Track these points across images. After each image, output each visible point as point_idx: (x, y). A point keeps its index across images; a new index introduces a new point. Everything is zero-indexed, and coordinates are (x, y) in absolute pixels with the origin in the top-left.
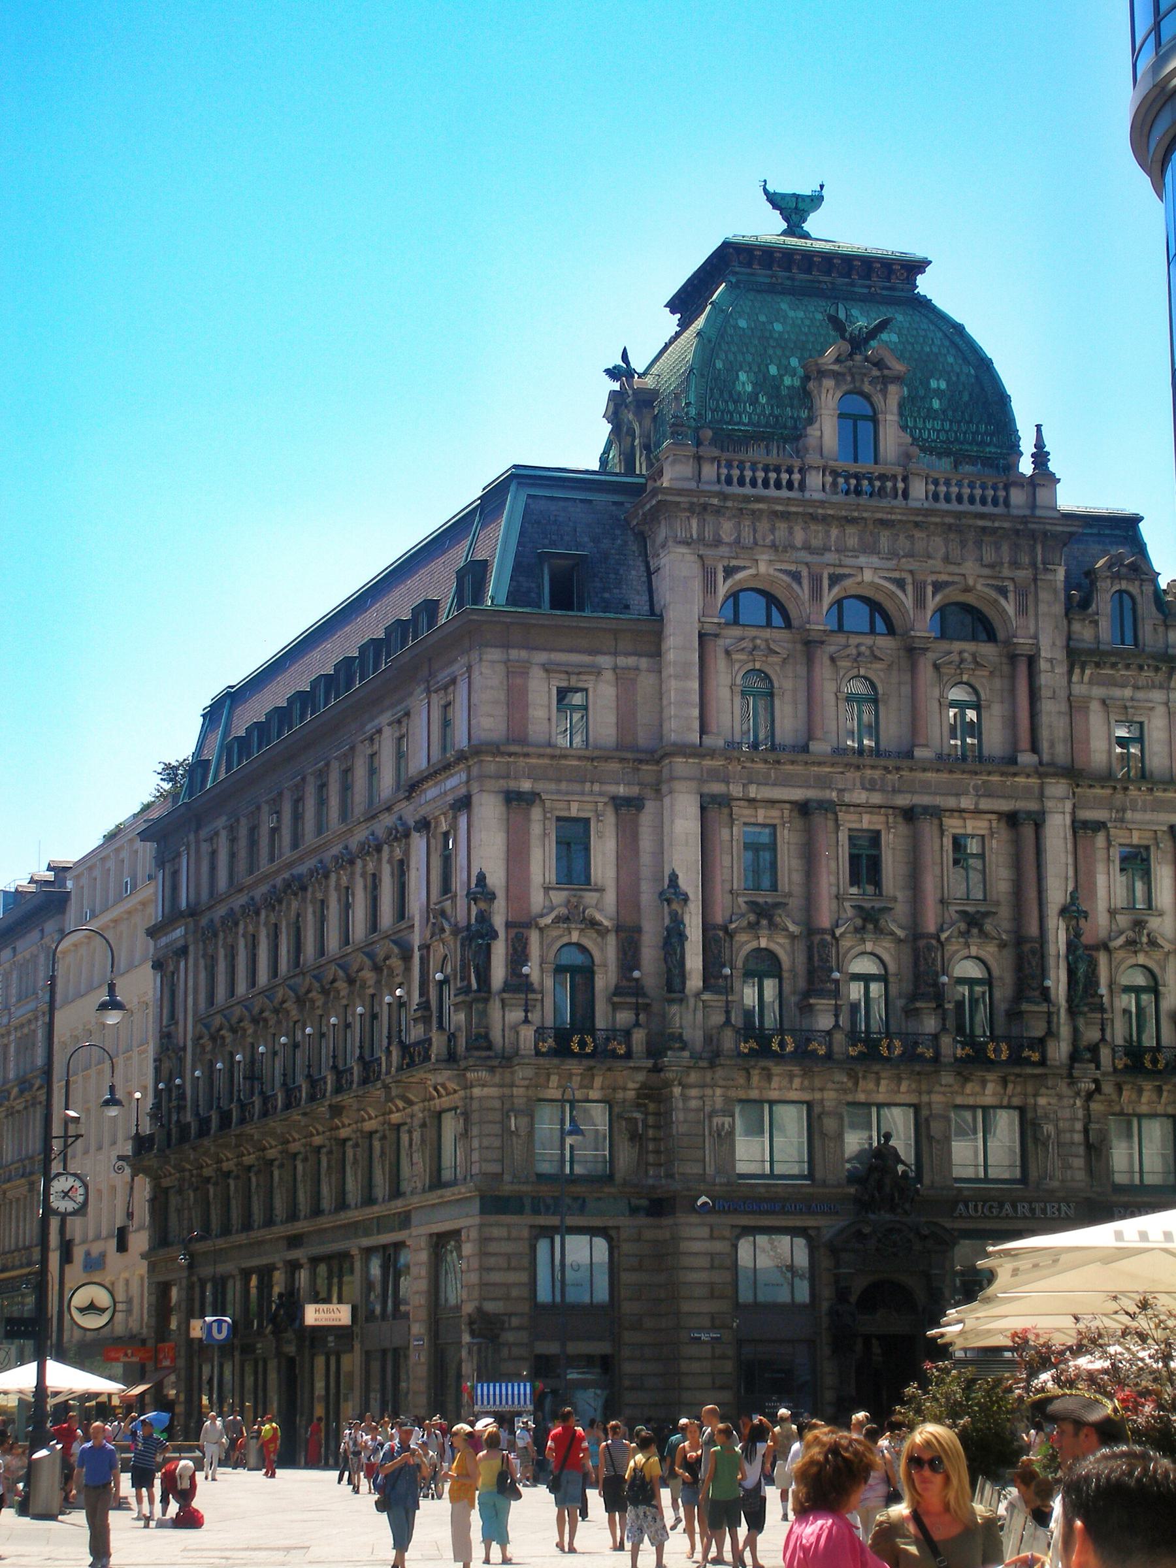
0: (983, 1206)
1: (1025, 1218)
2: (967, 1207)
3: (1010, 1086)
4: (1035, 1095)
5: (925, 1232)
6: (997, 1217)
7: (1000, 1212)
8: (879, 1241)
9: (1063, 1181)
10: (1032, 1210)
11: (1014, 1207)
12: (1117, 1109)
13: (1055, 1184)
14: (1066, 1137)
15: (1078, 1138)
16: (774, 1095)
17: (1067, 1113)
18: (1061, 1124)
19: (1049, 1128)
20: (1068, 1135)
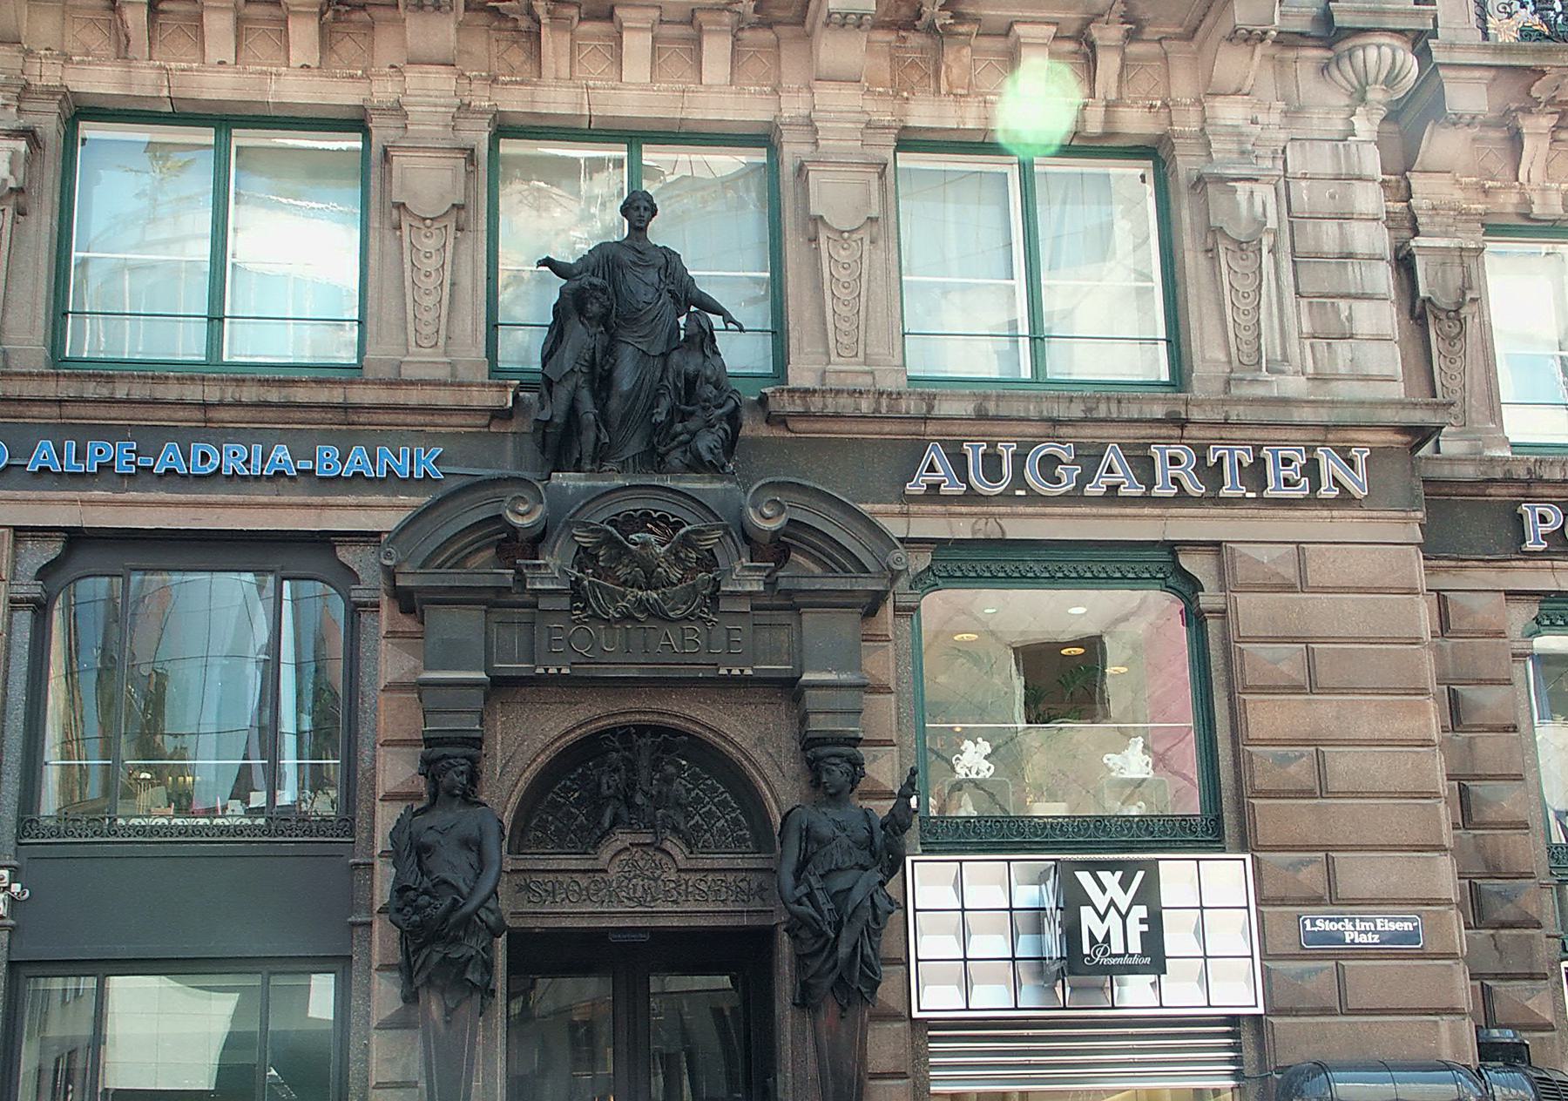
0: (1019, 459)
1: (1183, 498)
2: (959, 462)
3: (1108, 64)
4: (1210, 91)
5: (767, 522)
6: (1076, 497)
7: (1083, 480)
8: (585, 557)
9: (1318, 378)
10: (1212, 474)
11: (1143, 465)
12: (1508, 201)
13: (1292, 385)
14: (1328, 236)
15: (1372, 238)
16: (219, 83)
17: (1321, 161)
18: (1302, 193)
19: (1256, 201)
20: (1330, 227)
